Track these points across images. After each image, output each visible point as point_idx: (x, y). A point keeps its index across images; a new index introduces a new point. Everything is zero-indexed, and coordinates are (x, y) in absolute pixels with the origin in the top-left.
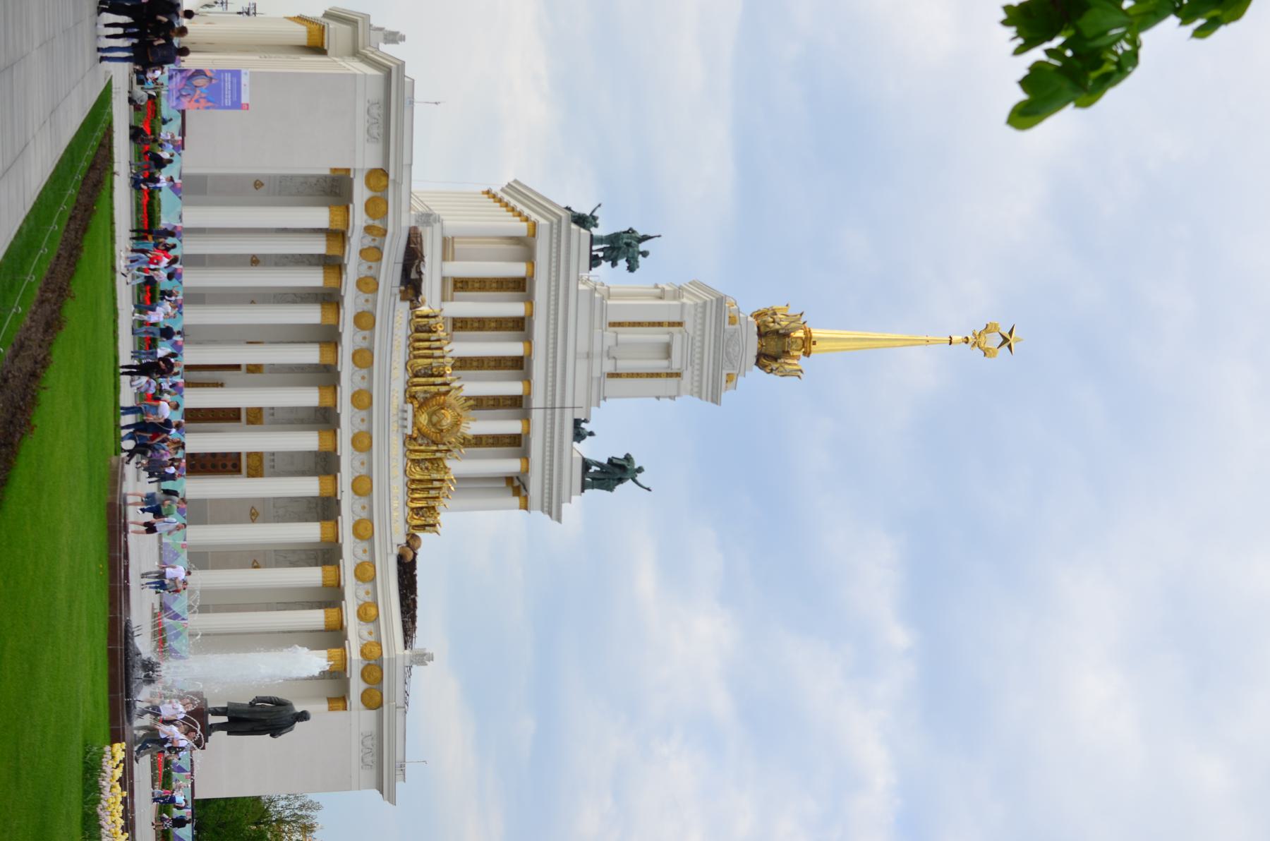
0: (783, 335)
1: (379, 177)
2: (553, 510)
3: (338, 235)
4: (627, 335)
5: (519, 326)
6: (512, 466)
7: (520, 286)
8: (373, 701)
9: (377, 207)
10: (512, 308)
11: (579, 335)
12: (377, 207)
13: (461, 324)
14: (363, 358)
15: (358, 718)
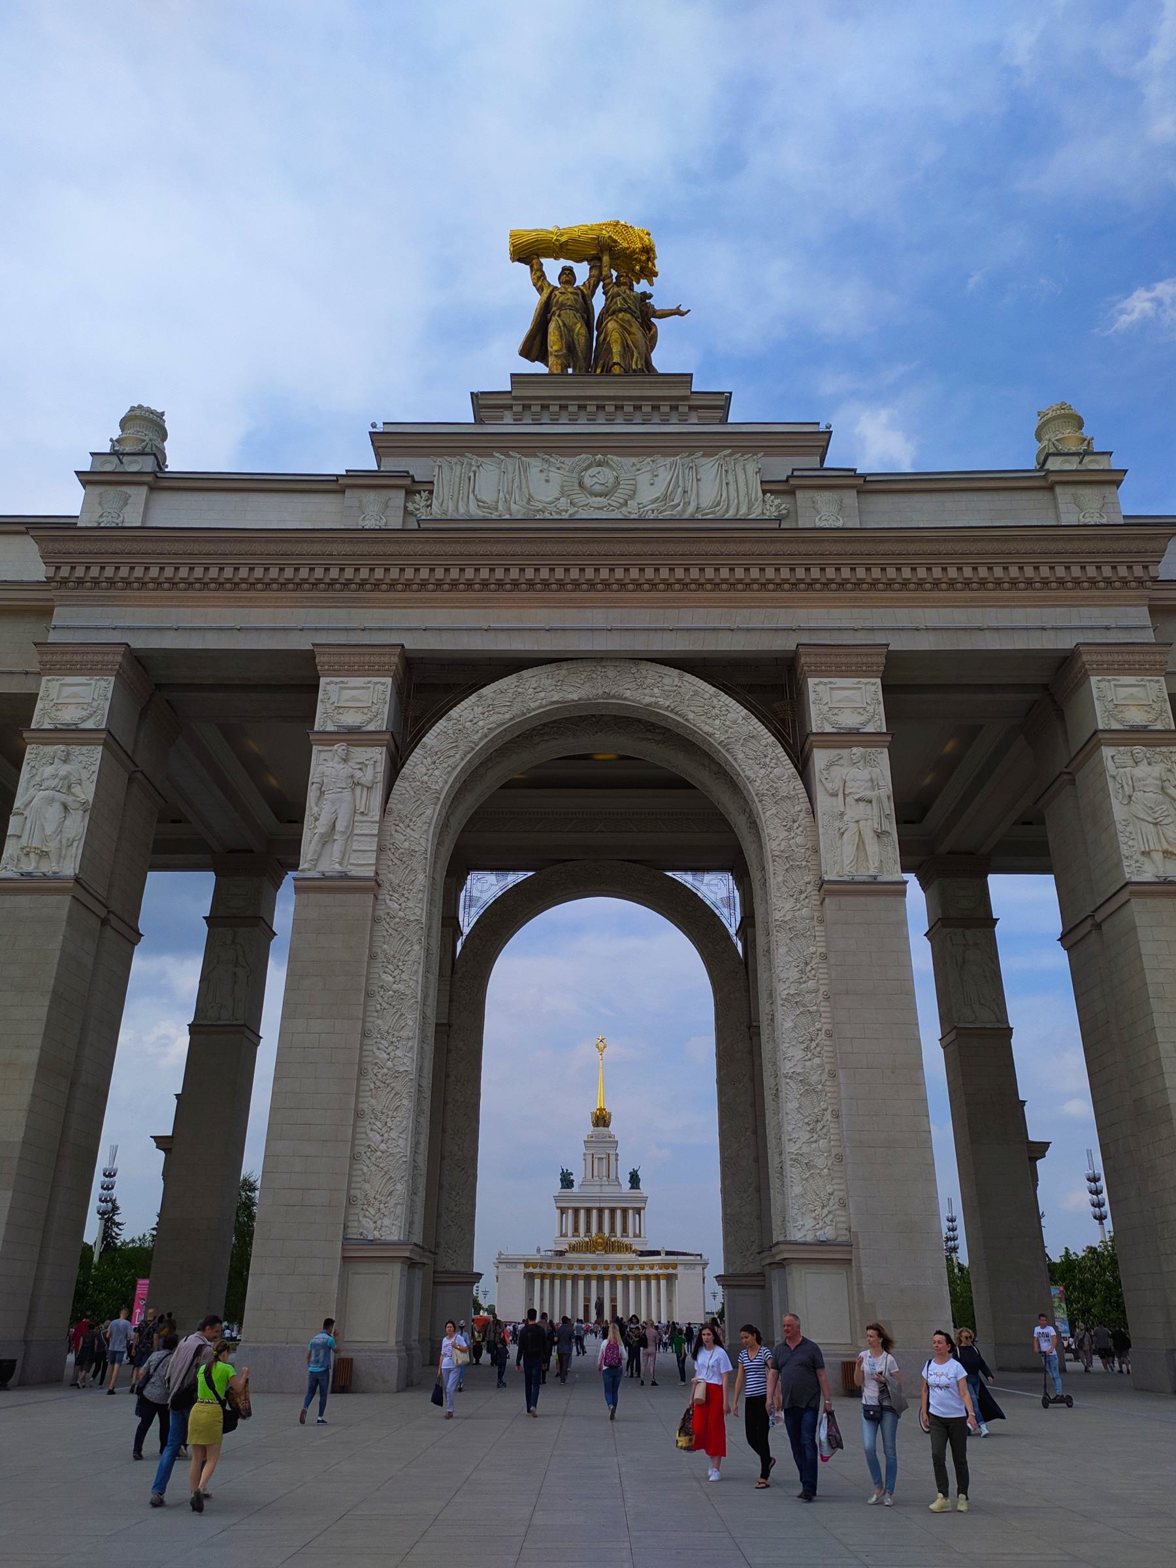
0: (597, 1117)
1: (527, 1265)
2: (644, 1199)
3: (543, 1277)
4: (596, 1174)
5: (588, 1211)
6: (631, 1212)
7: (576, 1211)
8: (675, 1266)
9: (534, 1265)
10: (582, 1213)
11: (594, 1191)
12: (534, 1265)
13: (588, 1229)
14: (582, 1267)
15: (680, 1271)
